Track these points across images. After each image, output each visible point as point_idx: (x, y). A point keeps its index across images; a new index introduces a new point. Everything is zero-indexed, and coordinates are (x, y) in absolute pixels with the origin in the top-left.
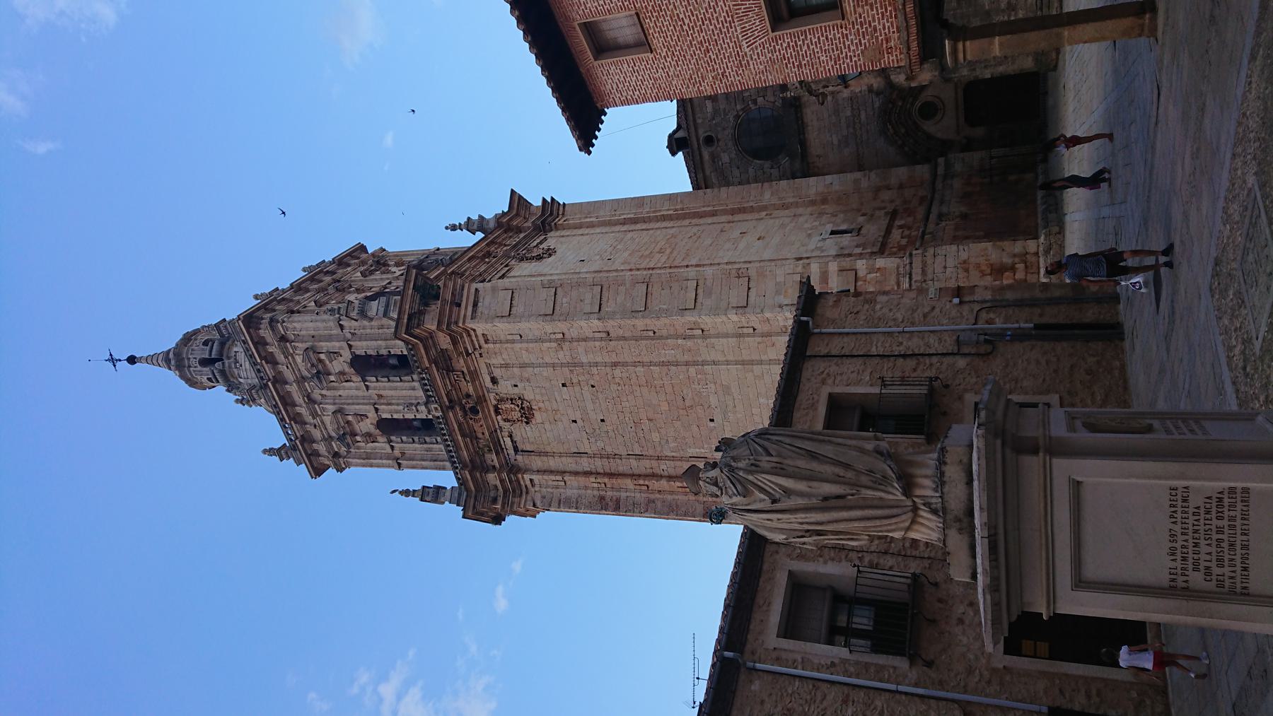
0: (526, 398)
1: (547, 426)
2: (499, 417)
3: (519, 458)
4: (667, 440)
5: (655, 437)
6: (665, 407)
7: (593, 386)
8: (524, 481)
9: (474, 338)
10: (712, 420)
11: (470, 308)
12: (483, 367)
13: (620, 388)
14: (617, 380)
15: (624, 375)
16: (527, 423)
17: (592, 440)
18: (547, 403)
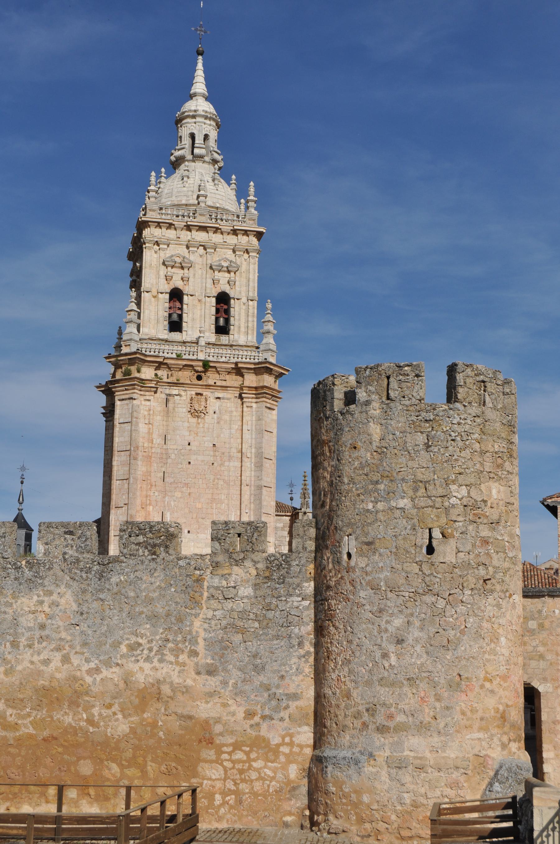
0: (206, 417)
1: (186, 424)
2: (194, 393)
3: (164, 396)
4: (175, 501)
5: (178, 494)
6: (199, 506)
7: (213, 464)
8: (149, 395)
9: (250, 400)
10: (189, 532)
11: (269, 405)
12: (229, 396)
13: (211, 481)
14: (216, 480)
15: (220, 486)
16: (189, 412)
17: (176, 452)
18: (202, 429)
